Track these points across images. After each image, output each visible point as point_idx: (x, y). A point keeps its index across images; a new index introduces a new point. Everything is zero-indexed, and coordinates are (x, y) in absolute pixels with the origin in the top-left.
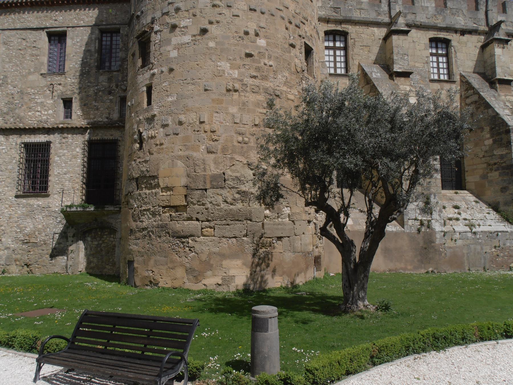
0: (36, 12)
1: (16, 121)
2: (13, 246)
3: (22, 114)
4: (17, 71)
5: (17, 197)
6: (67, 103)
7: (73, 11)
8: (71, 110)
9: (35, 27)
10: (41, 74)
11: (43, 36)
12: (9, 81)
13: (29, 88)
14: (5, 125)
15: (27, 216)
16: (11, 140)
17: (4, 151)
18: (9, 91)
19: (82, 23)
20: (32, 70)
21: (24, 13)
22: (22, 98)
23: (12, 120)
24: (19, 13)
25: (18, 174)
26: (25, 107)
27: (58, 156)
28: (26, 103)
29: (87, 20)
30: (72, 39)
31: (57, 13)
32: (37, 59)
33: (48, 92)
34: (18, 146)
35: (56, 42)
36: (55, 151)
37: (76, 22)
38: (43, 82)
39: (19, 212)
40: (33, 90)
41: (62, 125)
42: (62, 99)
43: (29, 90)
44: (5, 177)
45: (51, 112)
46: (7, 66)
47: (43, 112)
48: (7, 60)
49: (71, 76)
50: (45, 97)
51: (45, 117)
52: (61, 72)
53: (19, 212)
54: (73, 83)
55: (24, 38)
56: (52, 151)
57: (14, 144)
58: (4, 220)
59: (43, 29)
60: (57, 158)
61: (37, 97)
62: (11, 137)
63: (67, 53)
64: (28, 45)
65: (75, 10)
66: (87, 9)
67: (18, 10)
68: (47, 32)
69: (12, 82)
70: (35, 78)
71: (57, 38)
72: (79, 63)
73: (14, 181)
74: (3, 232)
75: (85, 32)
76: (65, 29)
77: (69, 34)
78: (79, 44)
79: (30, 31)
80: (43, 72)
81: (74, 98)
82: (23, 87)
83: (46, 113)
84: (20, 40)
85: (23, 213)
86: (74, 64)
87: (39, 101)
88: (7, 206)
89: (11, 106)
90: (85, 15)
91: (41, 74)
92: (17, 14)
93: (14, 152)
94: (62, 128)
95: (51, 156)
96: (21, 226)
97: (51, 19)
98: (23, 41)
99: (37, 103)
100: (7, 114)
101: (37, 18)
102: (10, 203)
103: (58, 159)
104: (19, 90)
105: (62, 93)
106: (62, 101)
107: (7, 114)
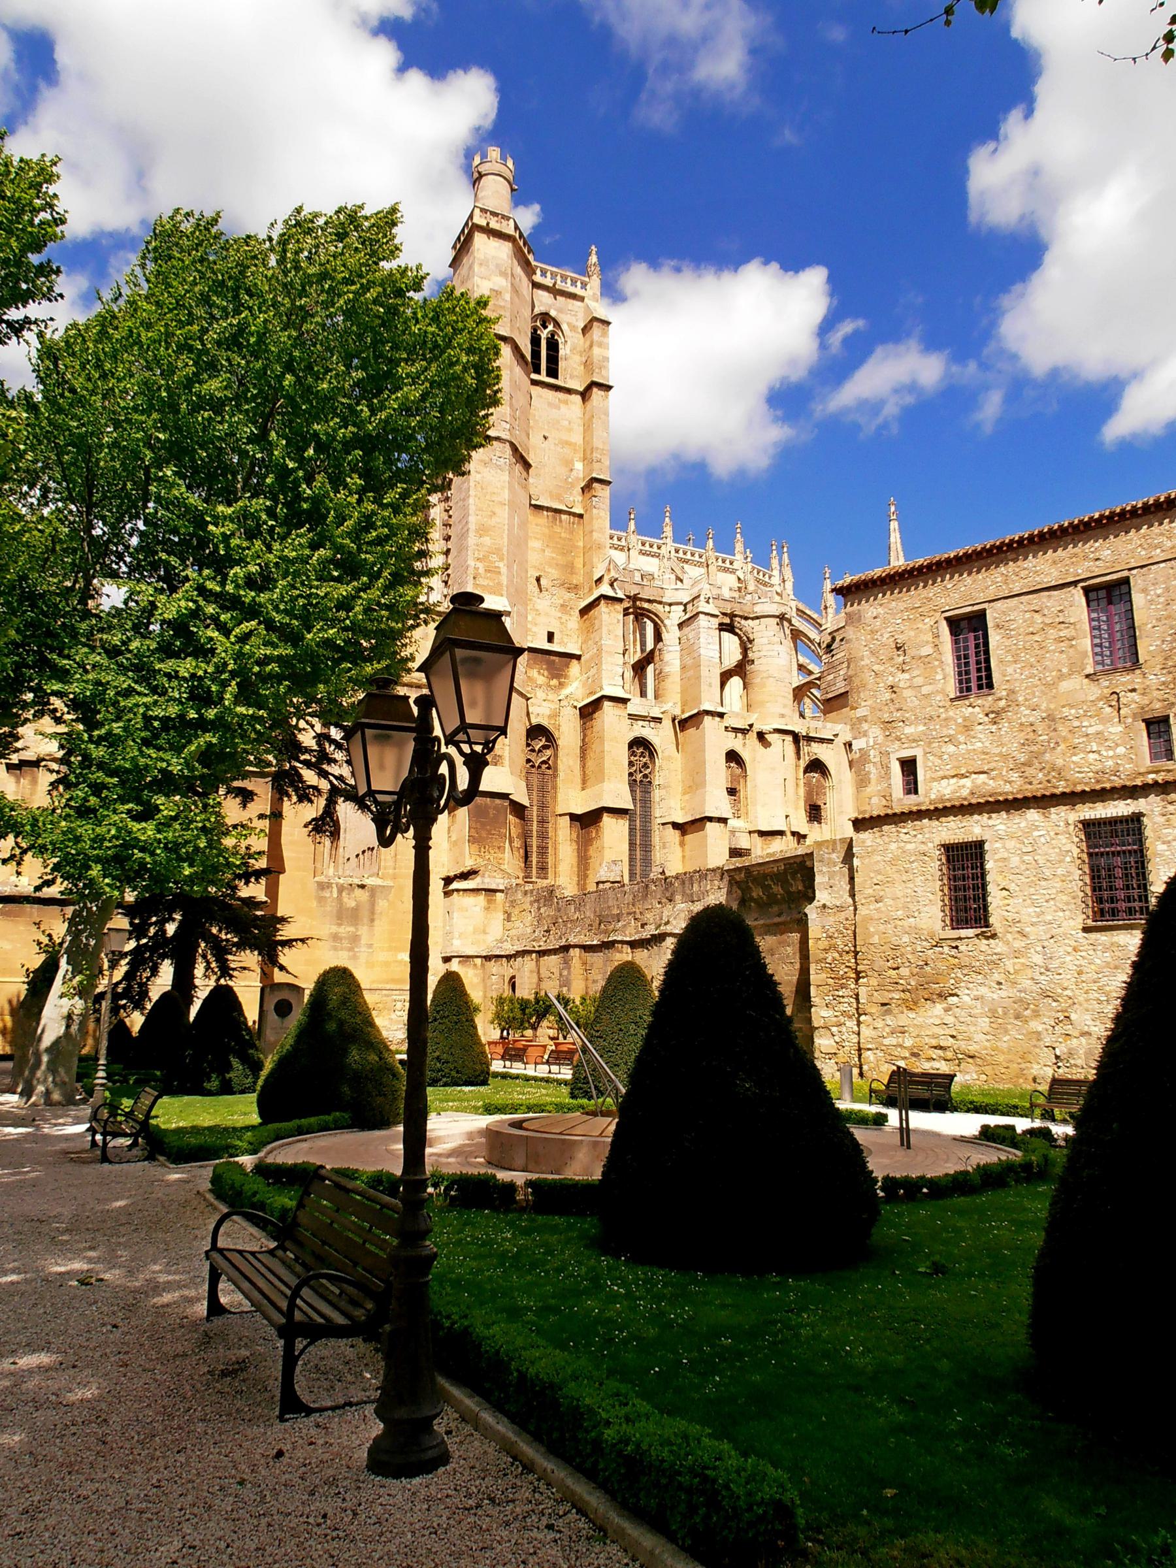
0: (1050, 551)
1: (1050, 777)
2: (1096, 1029)
3: (1060, 762)
4: (1033, 676)
5: (1086, 930)
6: (1157, 726)
7: (1133, 530)
8: (1169, 741)
9: (1053, 583)
10: (1087, 676)
11: (1076, 597)
12: (1021, 699)
13: (1063, 707)
14: (1030, 787)
15: (1116, 968)
16: (1053, 816)
17: (1043, 840)
18: (1024, 720)
19: (1158, 554)
20: (1065, 670)
21: (1026, 559)
22: (1055, 730)
23: (1040, 775)
24: (1015, 560)
25: (1081, 883)
26: (1062, 746)
27: (1164, 843)
28: (1065, 739)
29: (1169, 544)
30: (1144, 591)
31: (1097, 544)
32: (1072, 646)
33: (1109, 710)
34: (1072, 827)
35: (1103, 603)
36: (1155, 831)
37: (1143, 553)
38: (1094, 691)
39: (1098, 961)
40: (1073, 711)
41: (1153, 776)
42: (1144, 720)
43: (1066, 711)
44: (1054, 891)
45: (1121, 750)
46: (1010, 670)
47: (1105, 753)
48: (1009, 658)
49: (1157, 670)
50: (1104, 721)
51: (1110, 763)
52: (1135, 663)
53: (1098, 961)
54: (1164, 683)
55: (1036, 608)
56: (1148, 832)
57: (1062, 824)
58: (1069, 977)
59: (1074, 583)
60: (1161, 847)
61: (1085, 724)
62: (1053, 810)
63: (1136, 625)
64: (1048, 621)
65: (1138, 529)
66: (1167, 520)
67: (1014, 556)
68: (1083, 588)
69: (1026, 700)
70: (1074, 685)
71: (1102, 593)
72: (1169, 639)
73: (1074, 898)
74: (1070, 1001)
75: (1171, 571)
76: (1125, 574)
77: (1136, 583)
78: (1162, 600)
79: (1047, 593)
80: (1090, 670)
81: (1172, 715)
82: (1052, 706)
83: (1111, 753)
84: (1028, 615)
85: (1108, 963)
86: (1158, 643)
87: (1091, 730)
88: (1070, 949)
89: (1034, 748)
90: (1162, 534)
91: (1087, 676)
92: (1011, 563)
93: (1064, 841)
94: (1167, 783)
95: (1148, 843)
96: (1107, 988)
97: (1086, 558)
98: (1036, 616)
99: (1087, 735)
100: (1028, 764)
101: (1054, 562)
102: (1073, 943)
103: (1165, 847)
104: (1044, 715)
105: (1143, 708)
106: (1143, 725)
107: (1028, 764)
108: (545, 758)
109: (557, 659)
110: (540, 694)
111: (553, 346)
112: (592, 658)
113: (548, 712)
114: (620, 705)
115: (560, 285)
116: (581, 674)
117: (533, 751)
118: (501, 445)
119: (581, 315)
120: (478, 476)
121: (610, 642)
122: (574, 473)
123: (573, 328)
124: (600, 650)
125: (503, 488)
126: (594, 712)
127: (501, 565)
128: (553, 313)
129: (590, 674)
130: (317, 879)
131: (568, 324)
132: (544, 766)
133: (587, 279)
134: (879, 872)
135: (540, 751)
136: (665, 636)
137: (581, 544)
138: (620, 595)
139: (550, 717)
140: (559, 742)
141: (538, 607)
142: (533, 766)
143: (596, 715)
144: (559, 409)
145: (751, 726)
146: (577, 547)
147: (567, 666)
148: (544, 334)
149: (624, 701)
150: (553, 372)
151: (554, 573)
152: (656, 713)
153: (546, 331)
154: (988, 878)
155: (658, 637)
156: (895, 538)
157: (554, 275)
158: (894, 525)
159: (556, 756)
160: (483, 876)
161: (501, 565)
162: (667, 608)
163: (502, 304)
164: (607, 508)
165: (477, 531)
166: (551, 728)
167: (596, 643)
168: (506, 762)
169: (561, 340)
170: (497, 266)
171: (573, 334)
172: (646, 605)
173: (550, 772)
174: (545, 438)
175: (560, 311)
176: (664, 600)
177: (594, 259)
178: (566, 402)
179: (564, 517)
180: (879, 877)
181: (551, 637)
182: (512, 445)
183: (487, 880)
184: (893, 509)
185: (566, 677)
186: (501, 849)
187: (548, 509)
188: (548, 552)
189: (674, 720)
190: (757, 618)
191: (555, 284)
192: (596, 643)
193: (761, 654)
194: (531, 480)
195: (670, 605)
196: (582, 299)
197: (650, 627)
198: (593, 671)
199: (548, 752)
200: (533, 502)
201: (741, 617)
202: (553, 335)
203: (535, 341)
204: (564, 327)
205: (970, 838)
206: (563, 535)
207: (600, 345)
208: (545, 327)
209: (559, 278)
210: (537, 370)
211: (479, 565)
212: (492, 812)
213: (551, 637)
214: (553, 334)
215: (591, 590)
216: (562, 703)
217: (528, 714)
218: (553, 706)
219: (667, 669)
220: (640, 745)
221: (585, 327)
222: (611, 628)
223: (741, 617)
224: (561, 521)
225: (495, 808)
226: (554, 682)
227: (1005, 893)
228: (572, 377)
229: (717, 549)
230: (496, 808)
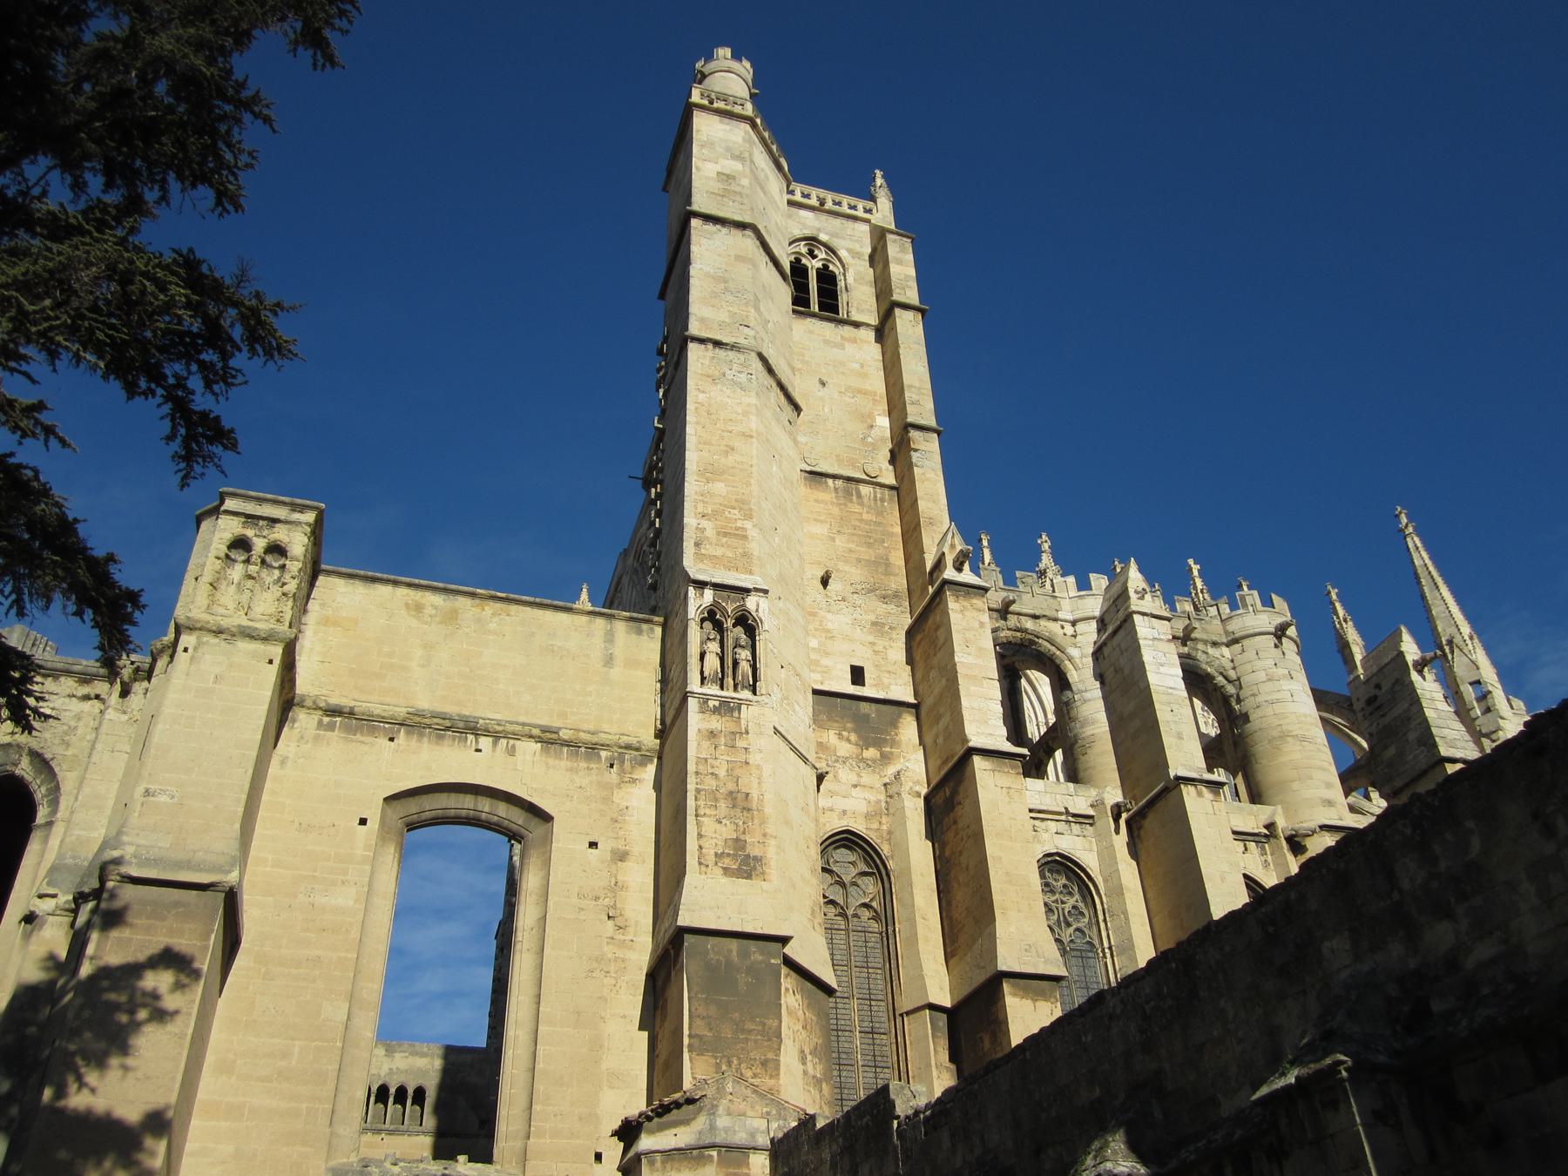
108: (867, 900)
110: (846, 775)
111: (827, 279)
113: (863, 808)
117: (842, 884)
118: (742, 357)
120: (701, 396)
122: (874, 433)
123: (855, 254)
125: (746, 413)
126: (955, 792)
127: (748, 525)
128: (823, 237)
130: (333, 1163)
131: (849, 251)
132: (866, 914)
133: (870, 205)
136: (1073, 676)
139: (868, 816)
140: (891, 864)
141: (830, 626)
143: (960, 797)
144: (844, 349)
145: (1270, 826)
146: (892, 535)
147: (894, 724)
148: (813, 265)
151: (856, 574)
152: (1081, 805)
155: (1061, 683)
156: (1421, 558)
158: (1414, 541)
159: (887, 893)
160: (713, 1112)
161: (748, 525)
162: (1069, 630)
163: (738, 189)
164: (939, 467)
165: (701, 473)
168: (773, 870)
170: (728, 149)
171: (856, 261)
172: (1029, 624)
173: (875, 926)
174: (823, 384)
176: (1061, 615)
177: (879, 181)
178: (854, 341)
179: (865, 490)
181: (857, 675)
182: (761, 357)
183: (722, 1122)
184: (1404, 520)
185: (894, 743)
186: (771, 1066)
187: (834, 477)
188: (841, 542)
189: (1116, 819)
190: (1236, 641)
193: (1260, 699)
195: (1074, 623)
197: (1038, 685)
198: (945, 720)
200: (808, 469)
201: (1205, 642)
202: (825, 267)
204: (843, 253)
206: (865, 516)
207: (900, 262)
211: (705, 523)
212: (743, 979)
213: (857, 675)
218: (873, 798)
219: (1088, 731)
220: (1059, 866)
221: (874, 250)
222: (969, 635)
223: (1205, 642)
224: (859, 496)
225: (750, 970)
226: (871, 753)
228: (859, 311)
230: (750, 970)
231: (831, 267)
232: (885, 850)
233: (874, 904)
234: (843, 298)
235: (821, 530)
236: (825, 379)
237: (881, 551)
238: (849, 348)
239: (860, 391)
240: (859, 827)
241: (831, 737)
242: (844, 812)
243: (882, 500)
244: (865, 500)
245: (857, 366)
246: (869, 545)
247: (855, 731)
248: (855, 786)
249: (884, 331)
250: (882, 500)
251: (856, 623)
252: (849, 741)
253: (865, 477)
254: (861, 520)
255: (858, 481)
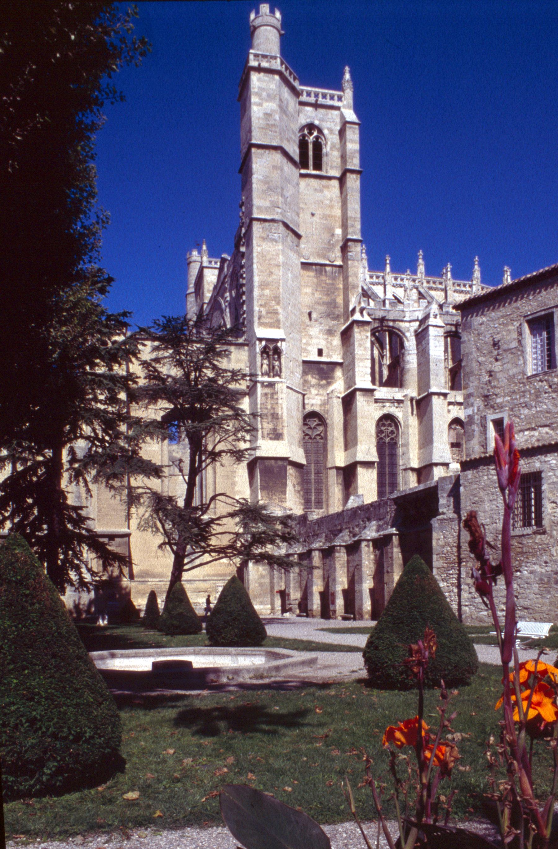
108: (318, 433)
109: (325, 367)
110: (314, 391)
111: (318, 147)
112: (349, 364)
114: (369, 394)
115: (321, 100)
116: (343, 375)
119: (338, 120)
121: (360, 352)
123: (331, 131)
124: (354, 358)
128: (317, 122)
129: (349, 374)
132: (318, 437)
133: (341, 93)
134: (475, 495)
135: (315, 428)
137: (341, 286)
138: (367, 318)
139: (321, 405)
140: (328, 421)
141: (311, 333)
142: (311, 438)
147: (333, 370)
149: (371, 391)
150: (318, 165)
151: (322, 308)
153: (311, 138)
154: (543, 495)
157: (316, 95)
159: (326, 431)
166: (322, 413)
167: (351, 354)
169: (323, 142)
173: (322, 441)
174: (313, 215)
175: (321, 120)
177: (347, 76)
178: (327, 187)
179: (328, 269)
180: (476, 499)
185: (333, 378)
188: (317, 295)
191: (317, 101)
192: (351, 354)
194: (302, 246)
196: (338, 108)
199: (321, 428)
203: (303, 144)
204: (326, 132)
205: (533, 470)
206: (328, 281)
208: (311, 134)
209: (320, 96)
210: (306, 167)
213: (320, 353)
214: (317, 138)
215: (347, 319)
216: (330, 396)
217: (304, 405)
218: (323, 398)
224: (326, 272)
226: (324, 382)
227: (554, 505)
228: (332, 167)
229: (455, 276)
231: (320, 140)
232: (326, 416)
233: (322, 434)
234: (324, 159)
235: (308, 290)
236: (314, 212)
237: (333, 297)
238: (326, 192)
239: (329, 216)
240: (317, 409)
241: (309, 377)
242: (312, 405)
243: (335, 272)
244: (328, 274)
245: (328, 202)
246: (328, 295)
247: (318, 374)
248: (317, 395)
249: (342, 180)
250: (335, 272)
251: (321, 330)
252: (315, 378)
253: (328, 262)
254: (326, 283)
255: (325, 265)
